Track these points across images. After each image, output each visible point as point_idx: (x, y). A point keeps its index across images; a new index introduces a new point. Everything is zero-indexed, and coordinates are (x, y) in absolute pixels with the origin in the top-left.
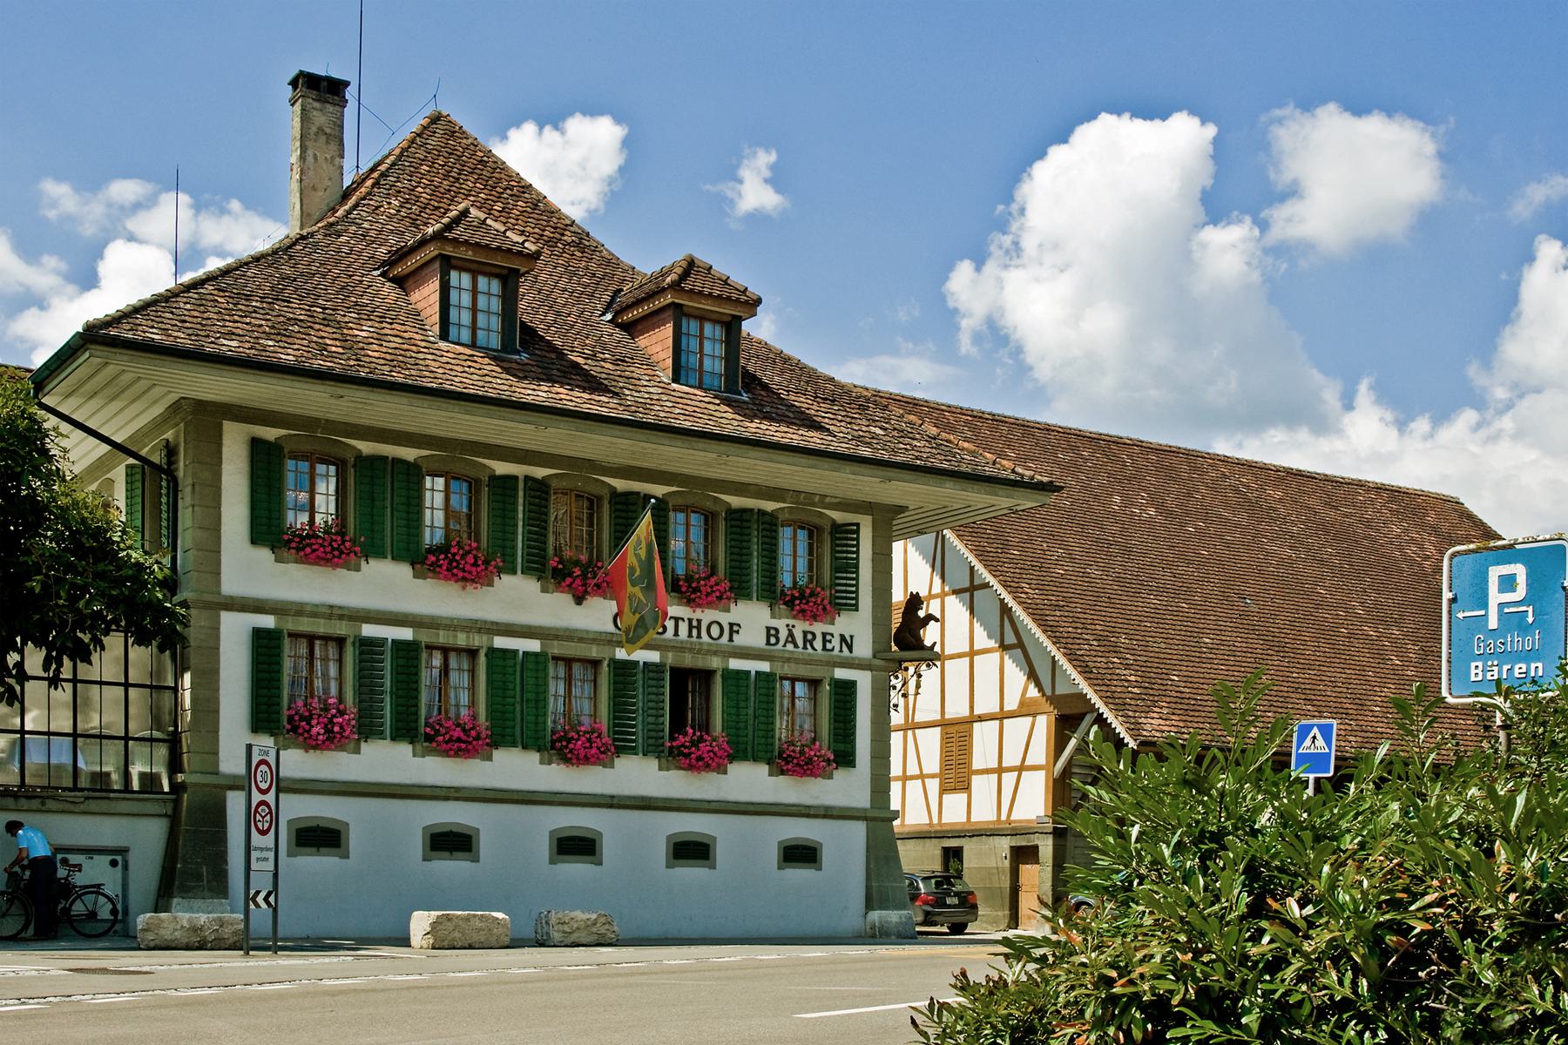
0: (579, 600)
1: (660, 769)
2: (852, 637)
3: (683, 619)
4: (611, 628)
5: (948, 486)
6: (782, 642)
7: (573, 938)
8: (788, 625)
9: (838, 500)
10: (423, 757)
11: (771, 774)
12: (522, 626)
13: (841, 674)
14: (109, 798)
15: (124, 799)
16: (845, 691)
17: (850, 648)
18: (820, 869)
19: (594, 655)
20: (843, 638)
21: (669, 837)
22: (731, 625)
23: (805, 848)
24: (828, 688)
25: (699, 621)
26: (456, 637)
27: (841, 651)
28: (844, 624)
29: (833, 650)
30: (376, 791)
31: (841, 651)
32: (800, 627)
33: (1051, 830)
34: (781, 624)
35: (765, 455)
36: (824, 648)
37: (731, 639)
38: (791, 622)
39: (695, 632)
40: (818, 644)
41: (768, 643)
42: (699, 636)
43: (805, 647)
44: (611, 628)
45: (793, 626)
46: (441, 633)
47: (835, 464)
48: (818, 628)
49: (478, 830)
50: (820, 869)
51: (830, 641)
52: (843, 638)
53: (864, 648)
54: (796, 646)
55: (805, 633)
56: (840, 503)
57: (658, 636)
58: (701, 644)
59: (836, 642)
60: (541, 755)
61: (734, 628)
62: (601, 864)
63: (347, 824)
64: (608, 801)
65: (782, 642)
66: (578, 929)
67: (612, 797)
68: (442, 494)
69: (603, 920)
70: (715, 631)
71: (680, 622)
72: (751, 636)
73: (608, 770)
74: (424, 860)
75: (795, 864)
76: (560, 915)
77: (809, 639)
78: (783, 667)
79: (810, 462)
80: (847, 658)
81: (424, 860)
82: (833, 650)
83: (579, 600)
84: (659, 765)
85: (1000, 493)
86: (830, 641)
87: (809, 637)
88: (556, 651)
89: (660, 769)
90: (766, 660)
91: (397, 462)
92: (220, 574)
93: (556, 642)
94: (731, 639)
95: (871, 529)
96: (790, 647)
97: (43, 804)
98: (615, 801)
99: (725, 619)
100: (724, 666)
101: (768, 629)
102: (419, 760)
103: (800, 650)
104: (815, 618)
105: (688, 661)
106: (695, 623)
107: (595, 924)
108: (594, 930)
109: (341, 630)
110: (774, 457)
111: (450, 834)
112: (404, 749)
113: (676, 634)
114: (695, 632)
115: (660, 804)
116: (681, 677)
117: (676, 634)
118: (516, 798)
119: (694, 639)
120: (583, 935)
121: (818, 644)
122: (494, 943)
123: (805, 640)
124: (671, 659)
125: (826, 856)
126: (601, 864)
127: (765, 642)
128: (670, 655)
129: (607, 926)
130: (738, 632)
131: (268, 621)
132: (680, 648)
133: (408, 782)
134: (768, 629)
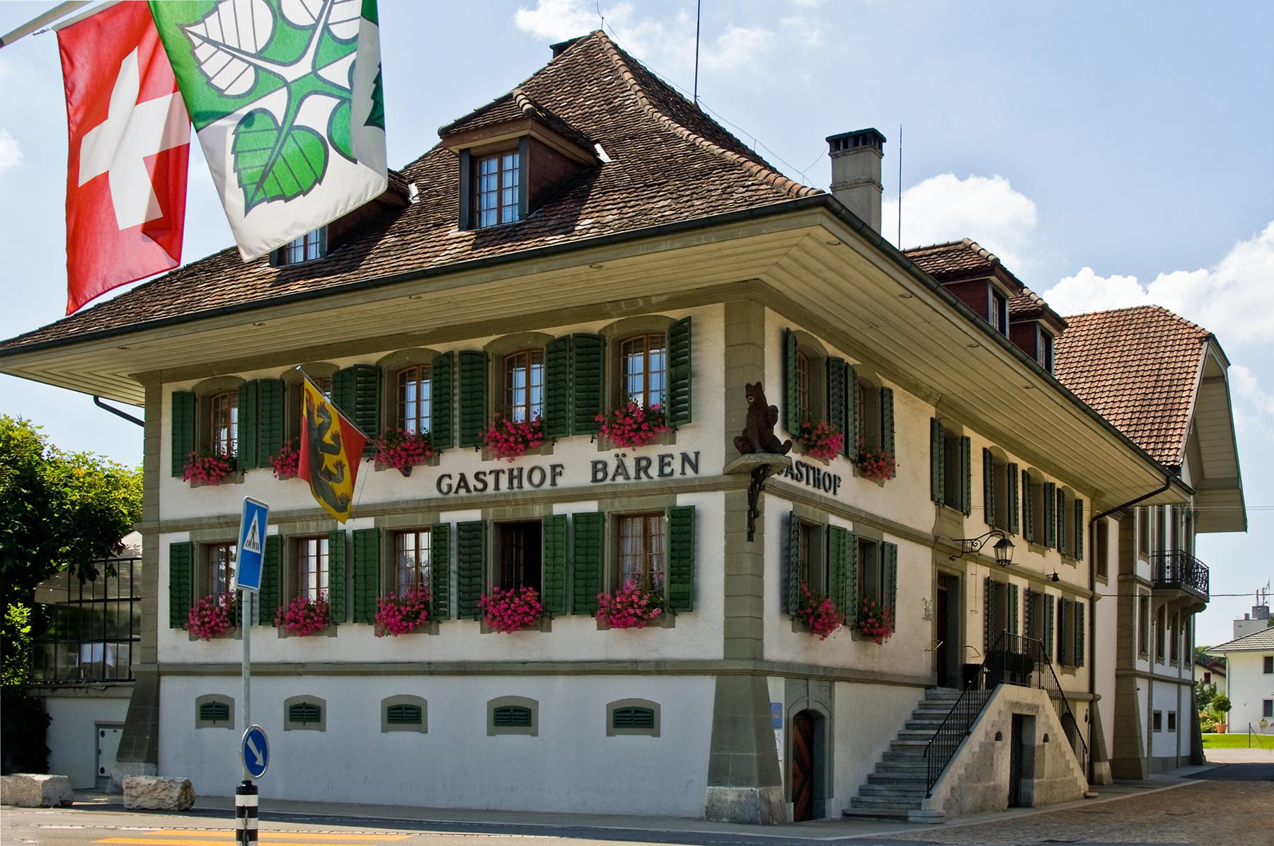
0: (406, 472)
1: (482, 632)
2: (697, 454)
3: (503, 472)
4: (436, 494)
5: (663, 247)
6: (610, 476)
7: (139, 802)
8: (617, 456)
9: (665, 297)
10: (286, 637)
11: (599, 628)
12: (300, 511)
13: (683, 500)
14: (117, 686)
15: (125, 686)
16: (685, 521)
17: (695, 468)
18: (657, 735)
19: (420, 523)
20: (685, 457)
21: (198, 699)
22: (553, 467)
23: (408, 708)
24: (667, 519)
25: (521, 470)
26: (308, 526)
27: (683, 473)
28: (686, 440)
29: (672, 473)
30: (413, 669)
31: (683, 473)
32: (631, 456)
33: (1196, 680)
34: (609, 456)
35: (446, 283)
36: (661, 474)
37: (554, 483)
38: (620, 451)
39: (515, 482)
40: (654, 471)
41: (595, 479)
42: (520, 486)
43: (638, 477)
44: (436, 494)
45: (624, 455)
46: (298, 524)
47: (521, 266)
48: (653, 452)
49: (659, 705)
50: (657, 735)
51: (669, 464)
52: (685, 457)
53: (713, 464)
54: (627, 478)
55: (638, 460)
56: (670, 300)
57: (479, 493)
58: (525, 493)
59: (676, 465)
60: (376, 628)
61: (556, 470)
62: (426, 732)
63: (325, 701)
64: (426, 668)
65: (610, 476)
66: (142, 793)
67: (429, 663)
68: (642, 377)
69: (162, 786)
70: (537, 477)
71: (501, 475)
72: (577, 475)
73: (546, 634)
74: (608, 735)
75: (406, 726)
76: (128, 780)
77: (642, 466)
78: (613, 503)
79: (492, 274)
80: (691, 480)
81: (608, 735)
82: (672, 473)
83: (406, 472)
84: (190, 636)
85: (741, 233)
86: (669, 464)
87: (644, 463)
88: (387, 526)
89: (482, 632)
90: (594, 499)
91: (269, 382)
92: (159, 505)
93: (387, 517)
94: (554, 483)
95: (722, 319)
96: (620, 480)
97: (87, 692)
98: (432, 668)
99: (545, 461)
100: (547, 513)
101: (595, 464)
102: (282, 640)
103: (633, 480)
104: (644, 442)
105: (510, 514)
106: (516, 473)
107: (155, 790)
108: (156, 795)
109: (229, 535)
110: (454, 282)
111: (305, 706)
112: (473, 628)
113: (497, 487)
114: (515, 482)
115: (475, 669)
116: (507, 530)
117: (497, 487)
118: (348, 670)
119: (516, 490)
120: (147, 799)
121: (654, 471)
122: (31, 803)
123: (638, 469)
124: (492, 514)
125: (666, 720)
126: (426, 732)
127: (590, 477)
128: (491, 511)
129: (166, 792)
130: (560, 474)
131: (184, 537)
132: (497, 502)
133: (275, 660)
134: (595, 464)
